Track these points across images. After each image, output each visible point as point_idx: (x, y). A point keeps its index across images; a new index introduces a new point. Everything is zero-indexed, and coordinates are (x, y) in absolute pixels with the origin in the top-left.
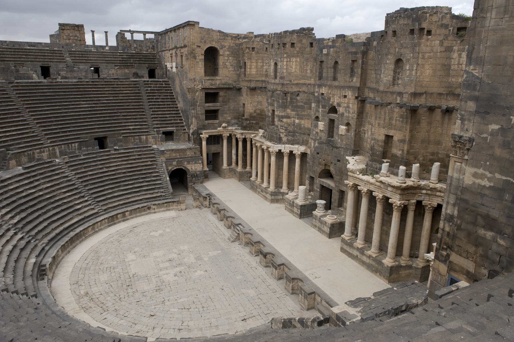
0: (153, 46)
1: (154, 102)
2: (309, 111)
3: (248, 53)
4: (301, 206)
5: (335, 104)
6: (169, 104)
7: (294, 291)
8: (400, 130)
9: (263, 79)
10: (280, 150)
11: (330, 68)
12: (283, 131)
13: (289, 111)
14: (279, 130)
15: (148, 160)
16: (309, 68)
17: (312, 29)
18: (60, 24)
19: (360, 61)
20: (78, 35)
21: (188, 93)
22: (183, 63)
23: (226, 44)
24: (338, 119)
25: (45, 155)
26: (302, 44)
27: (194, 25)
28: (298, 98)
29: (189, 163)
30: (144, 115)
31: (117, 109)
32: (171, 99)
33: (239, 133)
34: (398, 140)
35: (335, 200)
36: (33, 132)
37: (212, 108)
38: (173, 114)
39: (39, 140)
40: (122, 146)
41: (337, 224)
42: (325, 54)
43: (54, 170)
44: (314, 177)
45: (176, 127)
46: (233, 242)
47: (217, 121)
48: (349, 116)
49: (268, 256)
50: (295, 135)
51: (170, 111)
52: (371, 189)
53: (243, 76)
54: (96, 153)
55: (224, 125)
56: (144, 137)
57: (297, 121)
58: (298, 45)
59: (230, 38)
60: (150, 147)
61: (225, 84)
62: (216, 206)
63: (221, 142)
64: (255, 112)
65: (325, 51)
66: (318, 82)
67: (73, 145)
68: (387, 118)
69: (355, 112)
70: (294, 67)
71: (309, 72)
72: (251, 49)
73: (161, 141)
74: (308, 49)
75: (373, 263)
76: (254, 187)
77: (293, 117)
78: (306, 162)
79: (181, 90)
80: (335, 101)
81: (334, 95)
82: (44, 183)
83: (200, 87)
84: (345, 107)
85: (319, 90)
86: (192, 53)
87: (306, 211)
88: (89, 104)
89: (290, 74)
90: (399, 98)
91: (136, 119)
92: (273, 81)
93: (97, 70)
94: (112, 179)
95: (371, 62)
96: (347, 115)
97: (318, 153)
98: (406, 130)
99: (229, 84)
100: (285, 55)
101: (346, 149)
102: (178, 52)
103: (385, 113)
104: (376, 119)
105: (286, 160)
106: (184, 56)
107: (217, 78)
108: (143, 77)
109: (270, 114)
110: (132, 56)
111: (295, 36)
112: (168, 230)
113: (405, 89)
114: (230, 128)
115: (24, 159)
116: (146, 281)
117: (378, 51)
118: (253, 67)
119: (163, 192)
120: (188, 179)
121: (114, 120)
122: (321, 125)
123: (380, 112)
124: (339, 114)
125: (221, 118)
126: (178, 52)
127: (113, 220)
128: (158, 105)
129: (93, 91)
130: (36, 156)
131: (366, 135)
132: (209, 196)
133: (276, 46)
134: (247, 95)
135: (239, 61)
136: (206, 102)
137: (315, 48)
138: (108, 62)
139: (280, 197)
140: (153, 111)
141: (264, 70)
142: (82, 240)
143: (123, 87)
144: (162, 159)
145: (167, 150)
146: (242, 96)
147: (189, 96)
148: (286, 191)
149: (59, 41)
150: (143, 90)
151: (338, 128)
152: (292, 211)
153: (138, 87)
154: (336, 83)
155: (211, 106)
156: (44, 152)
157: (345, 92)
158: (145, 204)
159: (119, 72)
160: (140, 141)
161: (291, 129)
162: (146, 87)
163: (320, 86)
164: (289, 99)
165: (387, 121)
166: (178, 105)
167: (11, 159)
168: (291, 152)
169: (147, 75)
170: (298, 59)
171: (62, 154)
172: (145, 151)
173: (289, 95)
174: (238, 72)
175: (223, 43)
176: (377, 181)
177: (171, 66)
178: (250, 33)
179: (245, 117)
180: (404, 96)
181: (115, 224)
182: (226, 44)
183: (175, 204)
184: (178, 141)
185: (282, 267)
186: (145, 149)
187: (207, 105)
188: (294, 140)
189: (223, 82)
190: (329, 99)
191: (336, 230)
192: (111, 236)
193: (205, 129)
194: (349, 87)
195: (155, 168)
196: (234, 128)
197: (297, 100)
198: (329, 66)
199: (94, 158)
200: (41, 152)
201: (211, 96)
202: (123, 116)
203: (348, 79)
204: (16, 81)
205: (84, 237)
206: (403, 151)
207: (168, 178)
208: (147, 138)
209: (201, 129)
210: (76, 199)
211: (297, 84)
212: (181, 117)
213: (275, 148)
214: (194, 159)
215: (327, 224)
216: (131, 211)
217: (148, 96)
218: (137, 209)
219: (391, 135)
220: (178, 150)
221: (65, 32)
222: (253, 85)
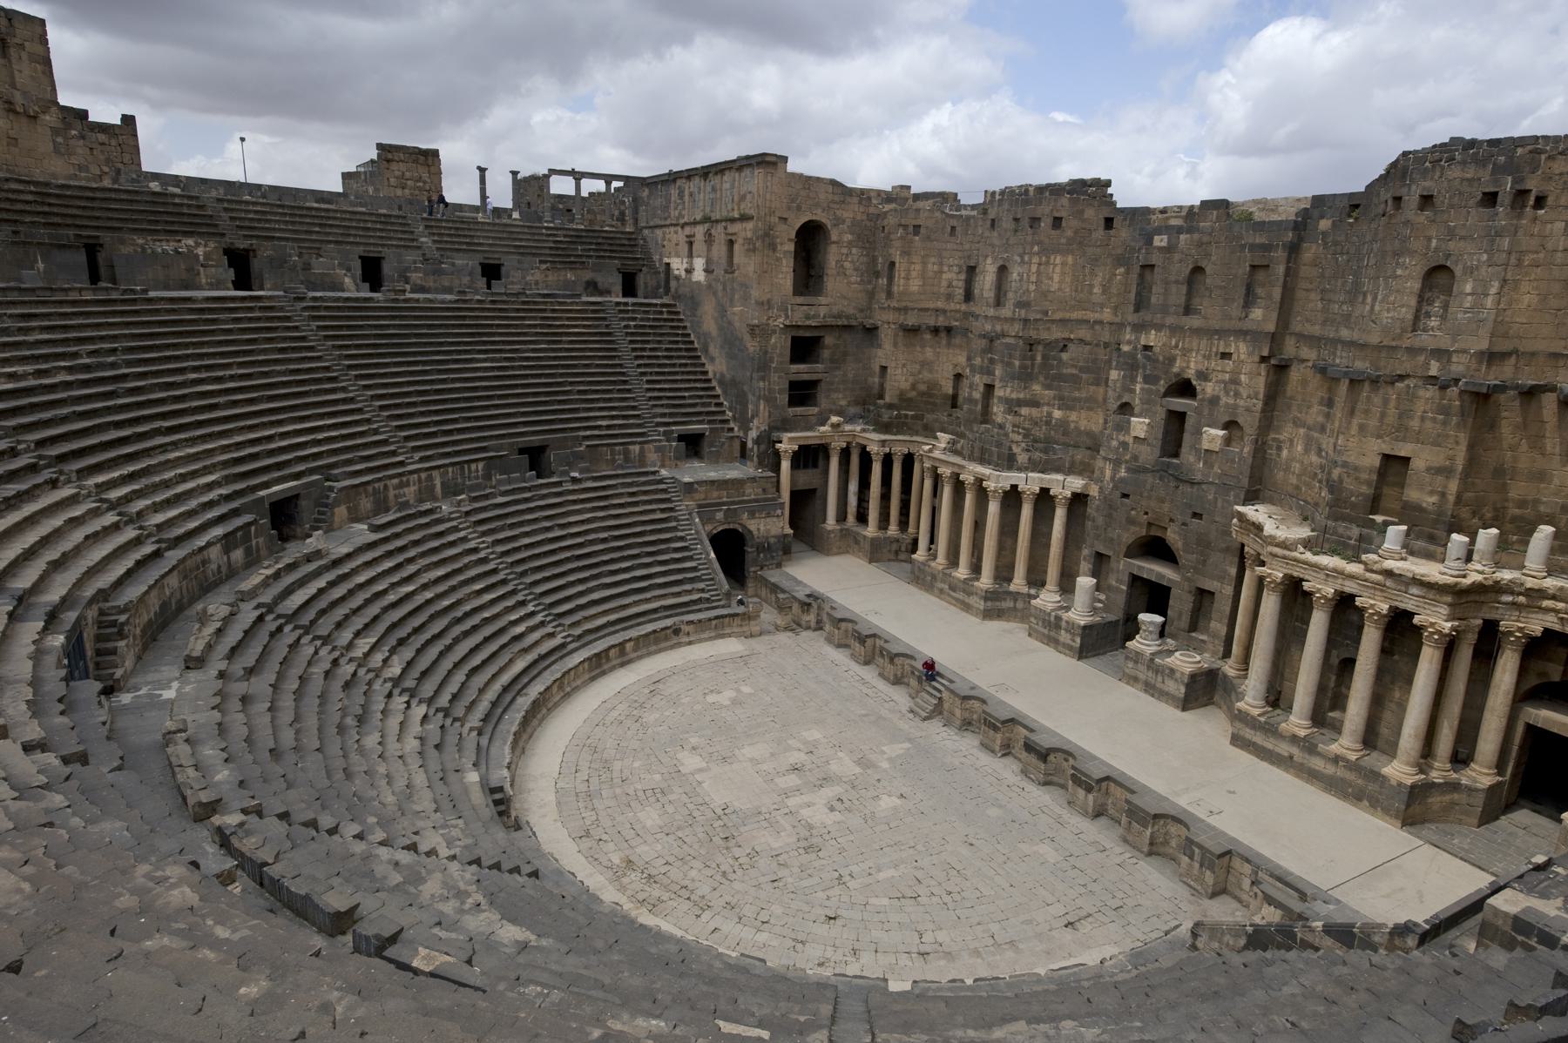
0: (622, 214)
1: (649, 357)
2: (1092, 388)
3: (902, 238)
4: (1085, 627)
5: (1190, 374)
6: (686, 365)
7: (1154, 849)
9: (940, 304)
10: (1014, 487)
11: (1177, 282)
12: (1019, 438)
13: (1037, 388)
14: (1006, 435)
15: (654, 507)
16: (1097, 281)
17: (1108, 183)
18: (380, 146)
19: (1281, 269)
20: (425, 176)
21: (747, 337)
22: (736, 260)
23: (847, 215)
25: (410, 492)
26: (1084, 221)
27: (774, 164)
28: (1065, 356)
29: (752, 514)
30: (629, 391)
31: (562, 375)
32: (687, 350)
33: (874, 441)
34: (1428, 469)
35: (1180, 614)
36: (376, 431)
37: (806, 377)
38: (697, 389)
39: (394, 453)
40: (588, 470)
41: (1202, 674)
42: (1160, 249)
43: (441, 534)
44: (1110, 553)
45: (710, 422)
46: (925, 719)
47: (815, 410)
48: (1236, 406)
49: (1051, 758)
50: (1077, 451)
51: (689, 381)
52: (1347, 590)
53: (883, 296)
54: (529, 489)
55: (834, 419)
56: (637, 448)
57: (1057, 414)
58: (1071, 224)
59: (856, 200)
60: (654, 473)
61: (839, 316)
62: (843, 625)
63: (821, 462)
64: (913, 387)
65: (1160, 241)
66: (1132, 318)
67: (473, 466)
68: (1392, 411)
69: (1257, 394)
70: (1056, 278)
72: (911, 229)
73: (677, 458)
74: (1100, 233)
76: (922, 579)
78: (1084, 516)
79: (721, 329)
80: (1190, 367)
81: (1186, 352)
82: (428, 568)
83: (780, 322)
84: (1223, 382)
85: (1138, 339)
86: (767, 235)
87: (1101, 641)
88: (492, 360)
89: (1045, 294)
91: (610, 400)
92: (991, 312)
93: (492, 272)
94: (579, 557)
95: (1304, 271)
96: (1231, 401)
97: (1125, 496)
98: (1457, 443)
99: (848, 317)
100: (1036, 248)
101: (1224, 488)
102: (718, 231)
103: (1386, 402)
105: (1027, 511)
106: (740, 241)
107: (822, 300)
108: (608, 292)
109: (977, 395)
110: (577, 237)
111: (1065, 200)
112: (746, 689)
113: (1454, 341)
114: (848, 428)
115: (366, 504)
116: (765, 824)
117: (1336, 243)
118: (914, 274)
119: (703, 591)
120: (749, 557)
121: (560, 402)
123: (1368, 398)
124: (1203, 400)
125: (824, 402)
126: (718, 231)
127: (599, 665)
128: (660, 366)
129: (498, 326)
130: (392, 493)
131: (1285, 453)
132: (812, 601)
133: (1007, 223)
134: (895, 345)
135: (874, 260)
136: (794, 360)
137: (1122, 233)
138: (523, 252)
139: (1009, 604)
140: (649, 382)
141: (944, 284)
142: (543, 718)
143: (568, 319)
144: (685, 505)
145: (700, 483)
146: (880, 346)
147: (752, 346)
148: (1025, 590)
149: (376, 190)
150: (617, 325)
152: (1053, 642)
153: (604, 319)
154: (1194, 322)
155: (802, 371)
156: (408, 484)
158: (668, 622)
159: (552, 277)
160: (627, 459)
161: (1040, 433)
162: (623, 319)
163: (1139, 328)
164: (1039, 358)
166: (709, 368)
167: (337, 503)
168: (1045, 492)
169: (618, 288)
170: (1070, 259)
171: (451, 490)
172: (644, 483)
173: (1040, 348)
174: (870, 287)
175: (839, 213)
176: (1368, 570)
177: (689, 267)
178: (902, 187)
179: (888, 399)
181: (604, 673)
182: (846, 215)
183: (737, 621)
184: (716, 459)
185: (1104, 784)
186: (643, 479)
187: (795, 367)
188: (1047, 461)
189: (835, 310)
190: (1172, 360)
191: (1204, 690)
192: (608, 705)
193: (786, 430)
194: (1242, 334)
195: (675, 529)
196: (858, 428)
197: (1060, 360)
198: (1173, 278)
199: (526, 500)
200: (401, 485)
201: (804, 347)
202: (579, 392)
203: (1235, 310)
204: (311, 294)
205: (544, 711)
206: (1443, 495)
207: (713, 555)
208: (642, 451)
209: (778, 429)
210: (509, 610)
211: (1063, 322)
212: (717, 396)
213: (998, 480)
214: (766, 507)
215: (1178, 675)
216: (637, 639)
217: (631, 342)
218: (647, 635)
219: (1402, 454)
220: (726, 482)
221: (394, 166)
222: (911, 320)
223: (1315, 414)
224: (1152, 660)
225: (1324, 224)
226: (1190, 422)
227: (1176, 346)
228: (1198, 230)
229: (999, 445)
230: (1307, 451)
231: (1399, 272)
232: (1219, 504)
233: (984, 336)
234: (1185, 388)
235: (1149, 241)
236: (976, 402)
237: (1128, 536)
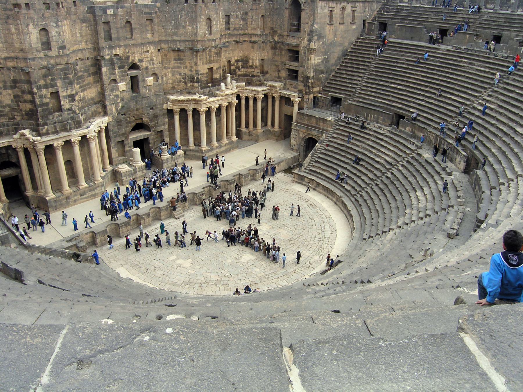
2: (88, 78)
5: (136, 61)
8: (217, 62)
14: (75, 112)
24: (142, 73)
28: (78, 67)
42: (111, 15)
44: (124, 139)
48: (154, 68)
57: (82, 94)
65: (110, 12)
68: (208, 57)
69: (159, 62)
71: (78, 35)
74: (73, 9)
75: (229, 146)
77: (79, 92)
80: (136, 58)
81: (133, 54)
85: (112, 53)
92: (42, 54)
104: (200, 60)
117: (164, 11)
122: (122, 86)
124: (143, 69)
131: (164, 78)
151: (144, 80)
157: (147, 48)
163: (111, 48)
165: (208, 59)
190: (128, 58)
194: (150, 43)
198: (119, 26)
223: (173, 63)
224: (172, 157)
225: (158, 5)
226: (140, 79)
227: (129, 52)
228: (125, 7)
229: (73, 118)
230: (173, 75)
232: (158, 101)
233: (43, 68)
234: (134, 66)
235: (105, 12)
236: (47, 104)
237: (129, 129)
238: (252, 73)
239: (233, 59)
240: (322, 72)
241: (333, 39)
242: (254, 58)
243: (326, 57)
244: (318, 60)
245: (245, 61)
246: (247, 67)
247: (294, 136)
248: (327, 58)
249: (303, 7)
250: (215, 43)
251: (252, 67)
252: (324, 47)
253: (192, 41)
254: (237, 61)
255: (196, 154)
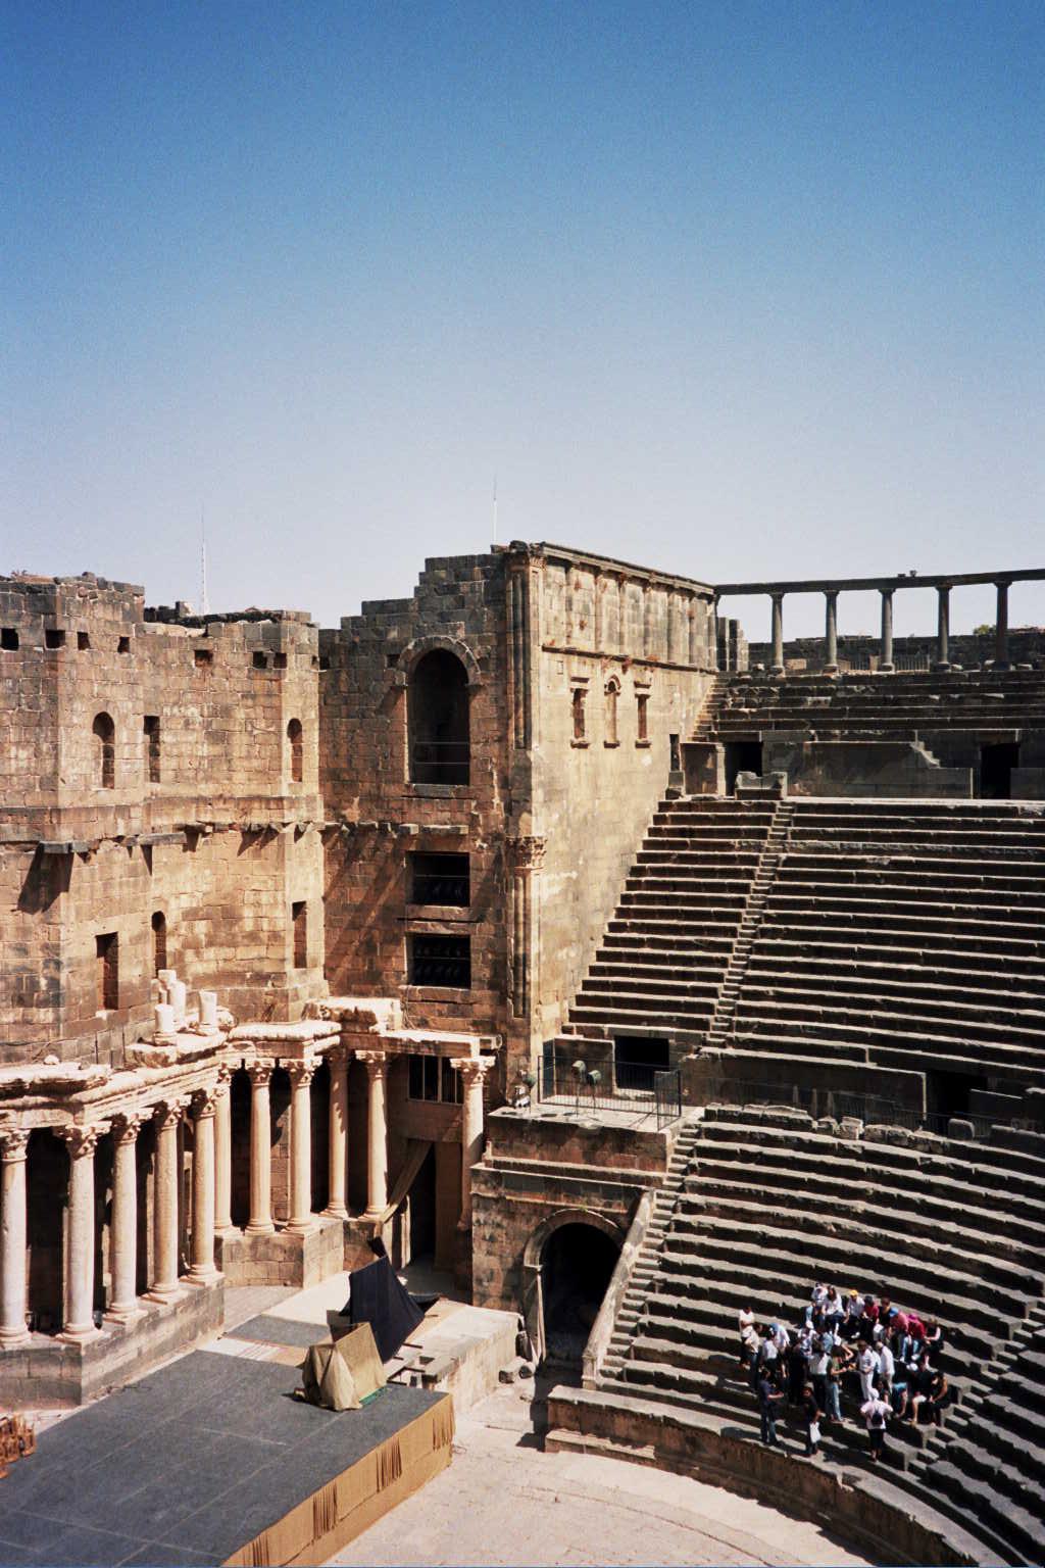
90: (121, 822)
103: (92, 876)
123: (79, 873)
165: (99, 895)
180: (132, 815)
231: (75, 720)
238: (257, 966)
239: (173, 903)
240: (566, 943)
241: (590, 805)
242: (264, 898)
243: (574, 875)
244: (551, 884)
245: (224, 916)
246: (235, 945)
247: (487, 1231)
248: (577, 882)
249: (475, 675)
250: (127, 826)
251: (253, 937)
252: (564, 837)
253: (33, 814)
254: (191, 915)
255: (39, 1371)
